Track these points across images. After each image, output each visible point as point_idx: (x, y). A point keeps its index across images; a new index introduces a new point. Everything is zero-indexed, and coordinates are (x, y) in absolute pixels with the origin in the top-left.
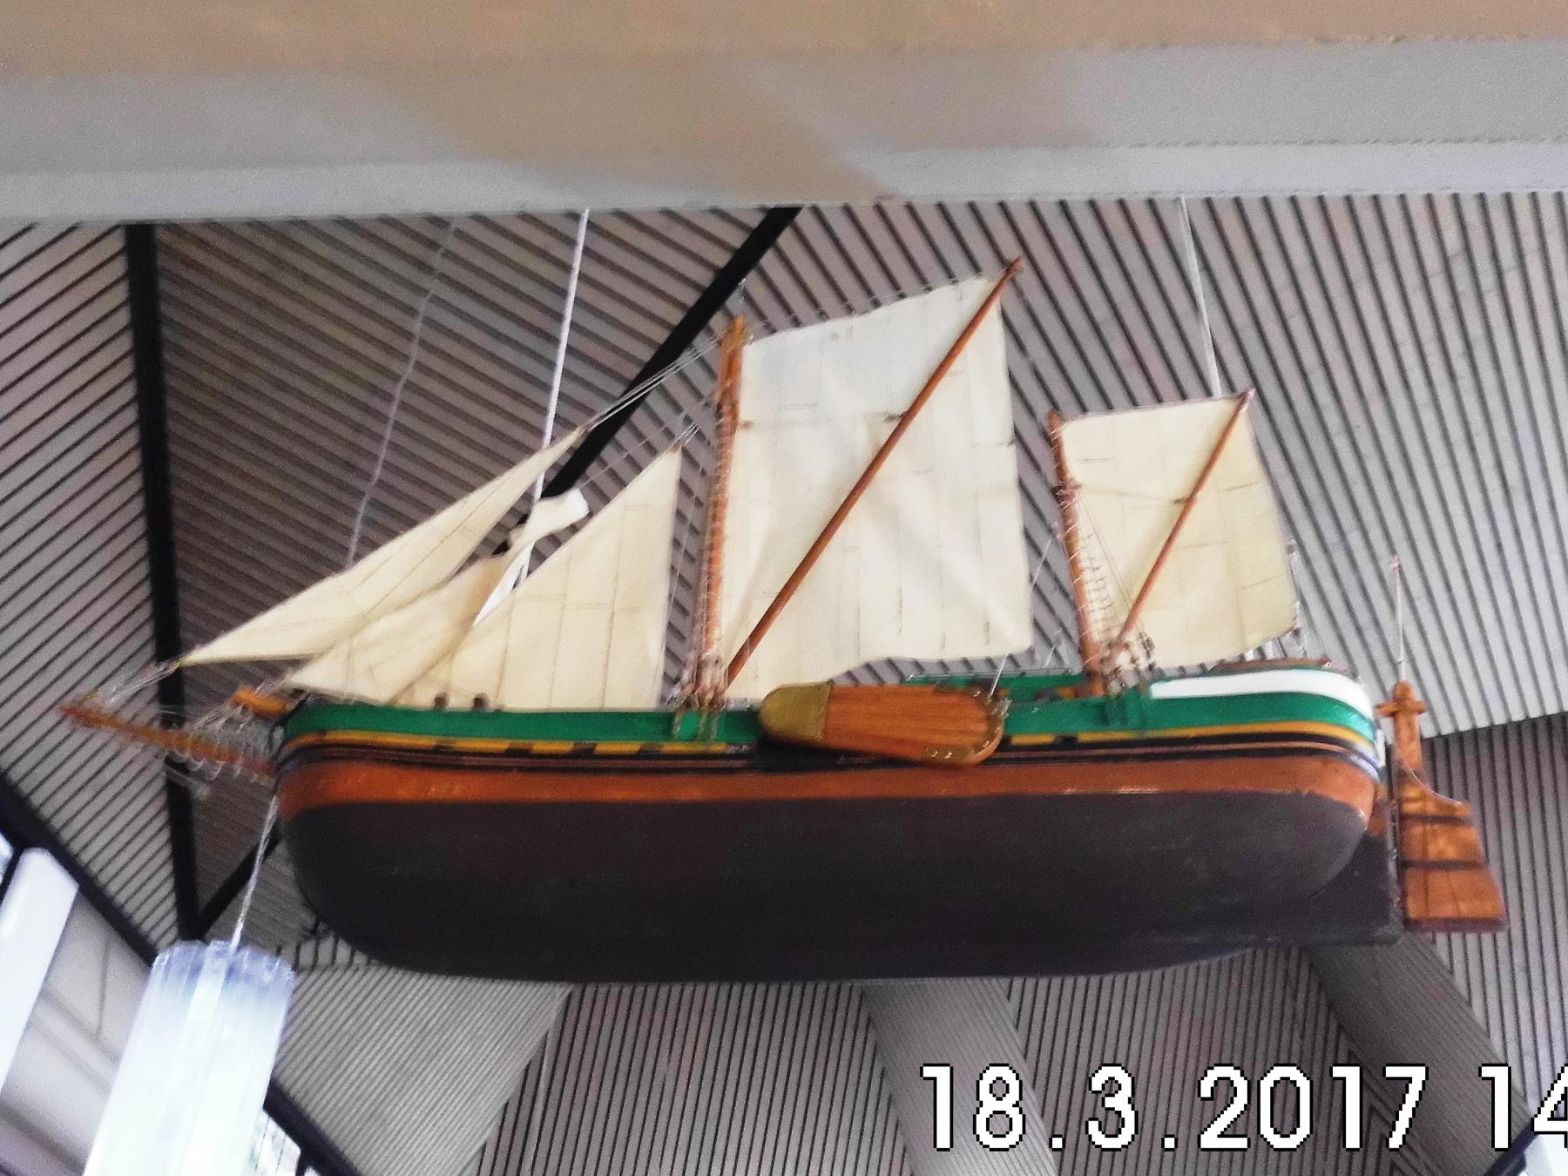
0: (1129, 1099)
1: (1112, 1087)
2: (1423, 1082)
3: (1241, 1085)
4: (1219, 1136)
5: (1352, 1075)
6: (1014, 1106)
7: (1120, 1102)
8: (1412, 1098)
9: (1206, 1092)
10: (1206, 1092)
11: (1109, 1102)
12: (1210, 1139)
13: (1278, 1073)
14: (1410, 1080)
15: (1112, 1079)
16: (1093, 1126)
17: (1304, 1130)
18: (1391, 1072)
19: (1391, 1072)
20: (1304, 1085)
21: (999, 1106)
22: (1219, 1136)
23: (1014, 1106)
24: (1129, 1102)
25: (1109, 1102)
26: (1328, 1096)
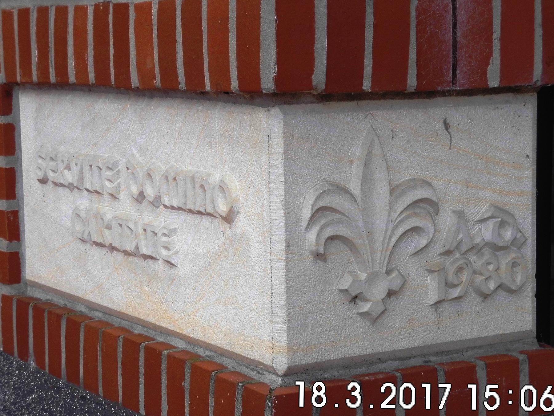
0: (359, 393)
1: (354, 389)
2: (486, 392)
3: (394, 389)
4: (387, 404)
5: (428, 386)
6: (323, 394)
7: (356, 393)
8: (447, 394)
9: (383, 391)
10: (383, 391)
11: (353, 393)
12: (384, 405)
13: (405, 385)
14: (446, 388)
15: (319, 386)
16: (348, 401)
17: (413, 403)
18: (440, 385)
19: (440, 386)
20: (413, 389)
21: (319, 394)
22: (387, 404)
23: (323, 394)
24: (359, 393)
25: (353, 393)
26: (421, 393)
